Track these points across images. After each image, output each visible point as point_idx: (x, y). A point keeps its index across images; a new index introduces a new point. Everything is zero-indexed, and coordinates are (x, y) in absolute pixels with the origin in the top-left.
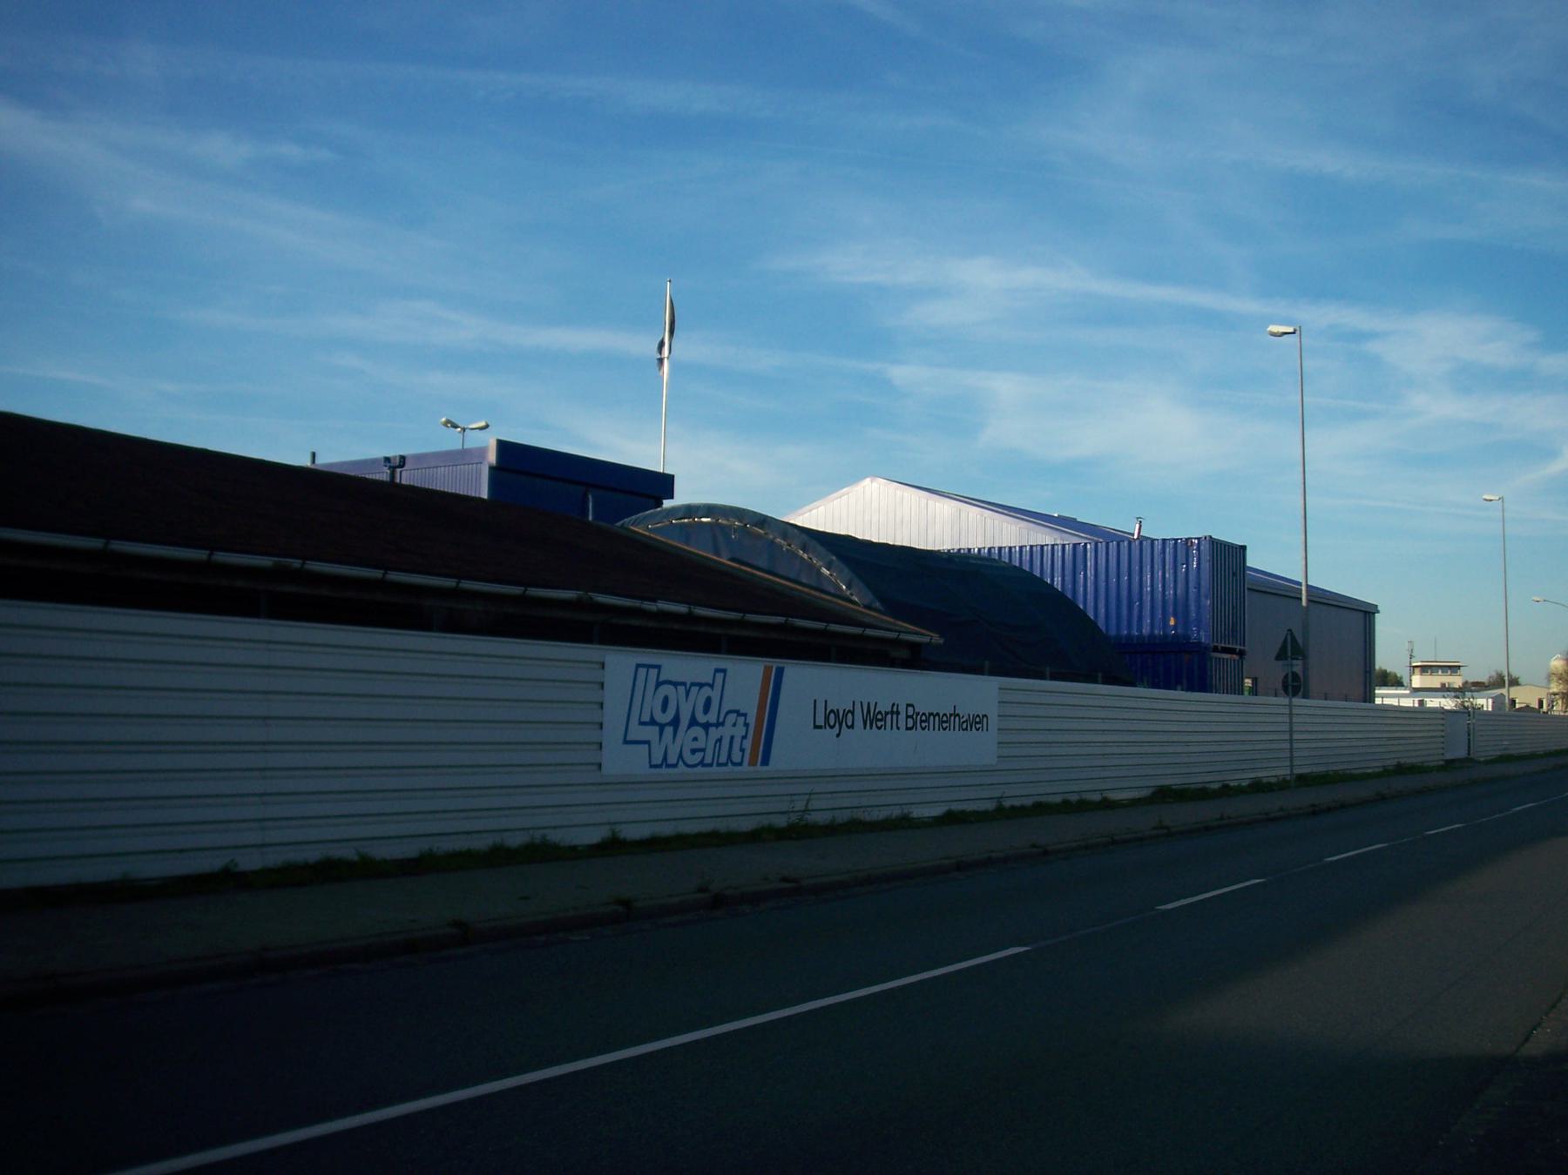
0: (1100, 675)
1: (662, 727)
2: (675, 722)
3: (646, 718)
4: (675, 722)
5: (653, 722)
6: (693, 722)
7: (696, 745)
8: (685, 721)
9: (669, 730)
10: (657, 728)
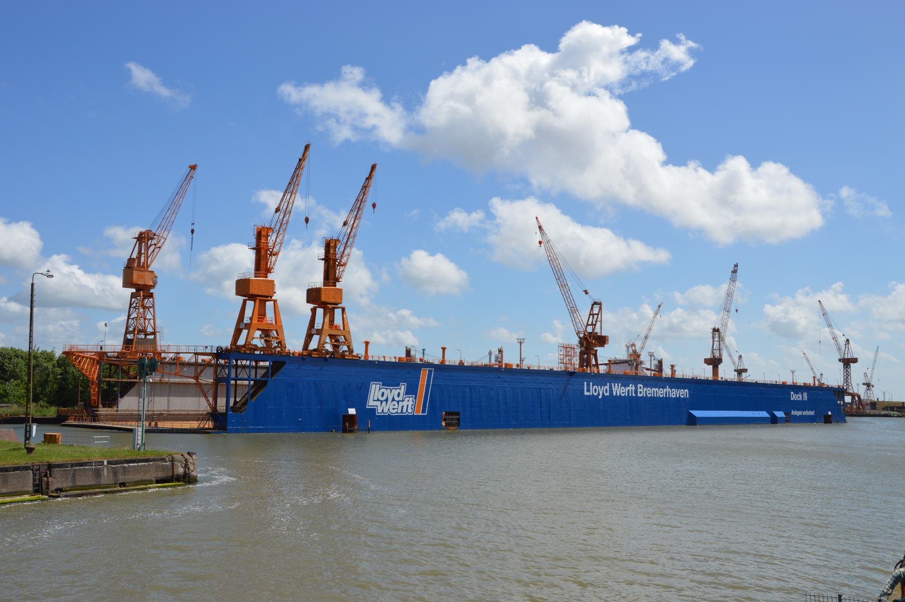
0: (668, 387)
1: (382, 402)
2: (387, 400)
3: (376, 399)
4: (387, 400)
5: (378, 400)
6: (393, 400)
8: (390, 399)
9: (384, 403)
10: (380, 402)
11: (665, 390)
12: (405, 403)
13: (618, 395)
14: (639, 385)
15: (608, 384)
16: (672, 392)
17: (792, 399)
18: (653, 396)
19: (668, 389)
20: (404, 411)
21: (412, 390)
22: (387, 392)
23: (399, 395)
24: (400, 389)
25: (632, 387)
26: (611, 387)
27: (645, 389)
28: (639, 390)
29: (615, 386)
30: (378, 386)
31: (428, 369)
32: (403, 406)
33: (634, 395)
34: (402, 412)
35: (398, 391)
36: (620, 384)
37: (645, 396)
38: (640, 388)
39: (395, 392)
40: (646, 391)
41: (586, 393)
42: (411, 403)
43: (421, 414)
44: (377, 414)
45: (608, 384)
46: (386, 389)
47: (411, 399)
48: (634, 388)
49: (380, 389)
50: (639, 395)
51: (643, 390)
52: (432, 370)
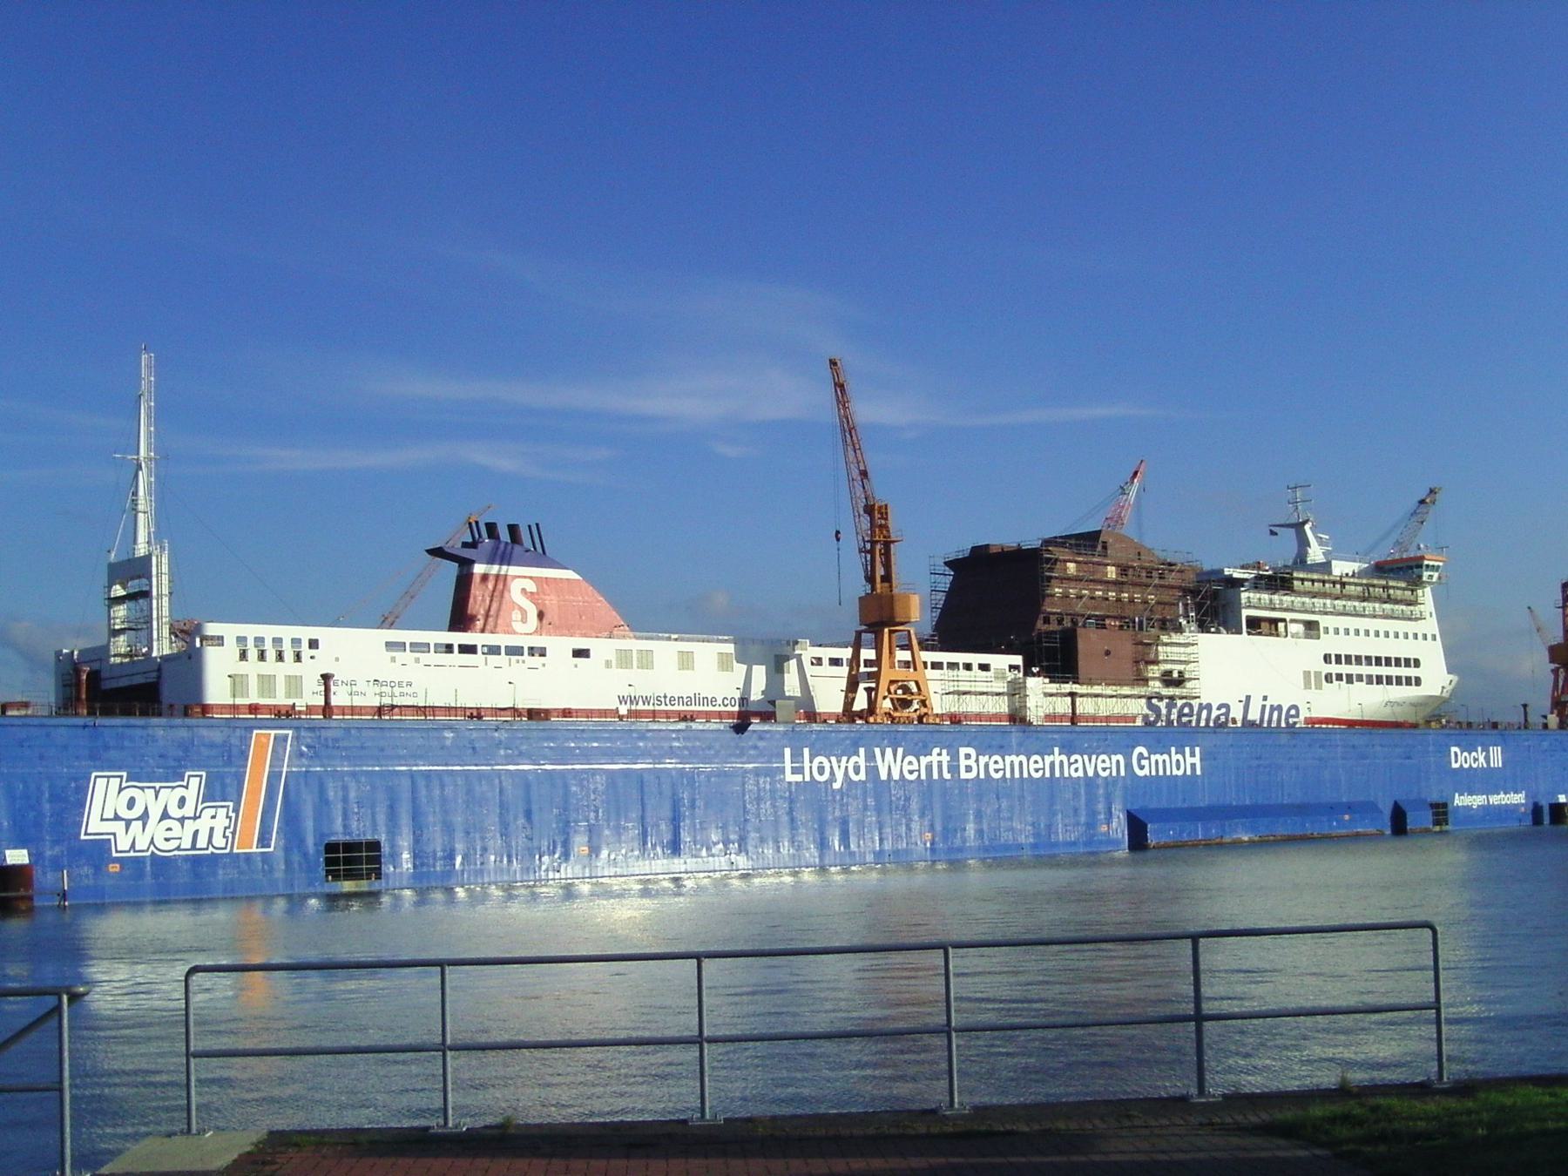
1: (128, 823)
2: (144, 817)
3: (109, 814)
4: (144, 817)
5: (117, 818)
6: (165, 815)
7: (169, 834)
8: (155, 814)
10: (123, 823)
11: (1048, 759)
12: (203, 825)
13: (896, 776)
14: (963, 751)
15: (862, 751)
16: (1070, 764)
17: (1455, 766)
18: (1008, 775)
19: (1057, 757)
20: (202, 842)
21: (220, 790)
22: (145, 797)
23: (182, 802)
24: (187, 787)
25: (940, 754)
26: (870, 757)
27: (983, 760)
28: (963, 763)
29: (883, 755)
30: (115, 783)
31: (273, 732)
32: (196, 833)
33: (947, 776)
34: (194, 847)
35: (180, 792)
36: (900, 751)
37: (982, 776)
38: (968, 756)
39: (170, 796)
40: (987, 766)
41: (790, 777)
42: (221, 822)
43: (254, 850)
44: (115, 855)
45: (862, 751)
46: (142, 788)
47: (222, 812)
48: (945, 758)
49: (121, 790)
50: (964, 775)
51: (977, 761)
52: (287, 736)
